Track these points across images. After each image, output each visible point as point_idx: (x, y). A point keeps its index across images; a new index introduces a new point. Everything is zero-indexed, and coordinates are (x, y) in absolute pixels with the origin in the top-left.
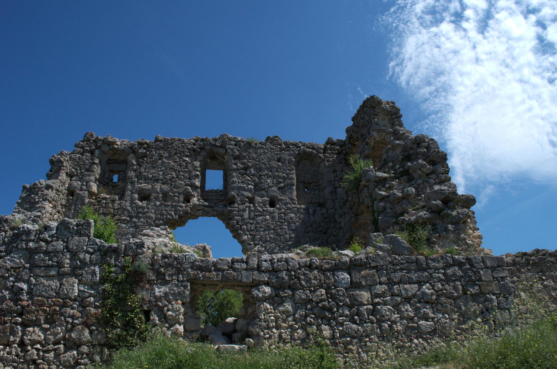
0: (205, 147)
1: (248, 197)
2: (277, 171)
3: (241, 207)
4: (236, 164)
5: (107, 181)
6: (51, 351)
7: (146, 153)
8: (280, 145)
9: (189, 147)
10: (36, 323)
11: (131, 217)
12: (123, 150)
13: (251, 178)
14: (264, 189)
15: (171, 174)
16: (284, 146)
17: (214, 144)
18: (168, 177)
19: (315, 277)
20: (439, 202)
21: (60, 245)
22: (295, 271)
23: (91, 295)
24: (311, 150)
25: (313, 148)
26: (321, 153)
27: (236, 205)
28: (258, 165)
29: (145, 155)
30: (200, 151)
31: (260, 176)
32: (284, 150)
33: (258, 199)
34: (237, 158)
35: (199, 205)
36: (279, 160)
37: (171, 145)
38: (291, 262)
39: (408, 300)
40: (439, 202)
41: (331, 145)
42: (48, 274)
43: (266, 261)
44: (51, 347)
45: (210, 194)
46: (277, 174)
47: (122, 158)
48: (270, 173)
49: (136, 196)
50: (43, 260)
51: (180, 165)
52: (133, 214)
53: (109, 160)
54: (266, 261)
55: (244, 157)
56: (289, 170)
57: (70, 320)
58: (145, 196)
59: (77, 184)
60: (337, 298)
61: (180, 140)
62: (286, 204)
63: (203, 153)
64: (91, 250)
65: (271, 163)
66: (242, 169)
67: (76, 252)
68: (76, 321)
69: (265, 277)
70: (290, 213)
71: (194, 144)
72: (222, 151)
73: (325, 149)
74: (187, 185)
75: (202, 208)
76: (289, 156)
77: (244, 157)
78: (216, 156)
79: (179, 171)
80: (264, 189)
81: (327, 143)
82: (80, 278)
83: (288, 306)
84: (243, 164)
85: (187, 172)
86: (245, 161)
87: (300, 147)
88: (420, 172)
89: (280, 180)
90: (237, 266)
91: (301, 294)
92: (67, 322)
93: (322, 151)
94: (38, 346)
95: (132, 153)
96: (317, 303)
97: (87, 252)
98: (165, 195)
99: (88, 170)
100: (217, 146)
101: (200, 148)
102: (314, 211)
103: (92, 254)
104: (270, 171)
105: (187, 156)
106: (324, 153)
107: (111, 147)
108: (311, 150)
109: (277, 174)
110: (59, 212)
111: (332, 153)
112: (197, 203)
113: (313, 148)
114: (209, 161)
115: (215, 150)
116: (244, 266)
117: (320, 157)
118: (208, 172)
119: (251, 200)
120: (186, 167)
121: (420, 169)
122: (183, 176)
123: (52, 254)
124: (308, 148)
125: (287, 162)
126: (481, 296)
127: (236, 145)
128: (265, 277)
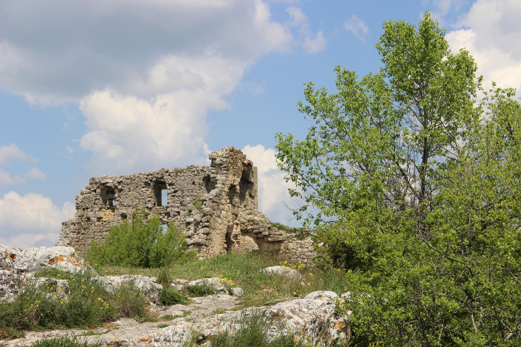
1: (177, 212)
2: (192, 192)
3: (173, 219)
9: (144, 181)
16: (196, 172)
27: (170, 218)
33: (182, 213)
36: (194, 183)
46: (192, 194)
49: (120, 218)
58: (124, 216)
59: (90, 214)
66: (173, 193)
84: (174, 189)
86: (174, 187)
89: (194, 198)
99: (94, 204)
105: (143, 187)
107: (105, 185)
109: (192, 194)
110: (83, 234)
114: (160, 185)
115: (159, 180)
119: (179, 213)
127: (169, 175)
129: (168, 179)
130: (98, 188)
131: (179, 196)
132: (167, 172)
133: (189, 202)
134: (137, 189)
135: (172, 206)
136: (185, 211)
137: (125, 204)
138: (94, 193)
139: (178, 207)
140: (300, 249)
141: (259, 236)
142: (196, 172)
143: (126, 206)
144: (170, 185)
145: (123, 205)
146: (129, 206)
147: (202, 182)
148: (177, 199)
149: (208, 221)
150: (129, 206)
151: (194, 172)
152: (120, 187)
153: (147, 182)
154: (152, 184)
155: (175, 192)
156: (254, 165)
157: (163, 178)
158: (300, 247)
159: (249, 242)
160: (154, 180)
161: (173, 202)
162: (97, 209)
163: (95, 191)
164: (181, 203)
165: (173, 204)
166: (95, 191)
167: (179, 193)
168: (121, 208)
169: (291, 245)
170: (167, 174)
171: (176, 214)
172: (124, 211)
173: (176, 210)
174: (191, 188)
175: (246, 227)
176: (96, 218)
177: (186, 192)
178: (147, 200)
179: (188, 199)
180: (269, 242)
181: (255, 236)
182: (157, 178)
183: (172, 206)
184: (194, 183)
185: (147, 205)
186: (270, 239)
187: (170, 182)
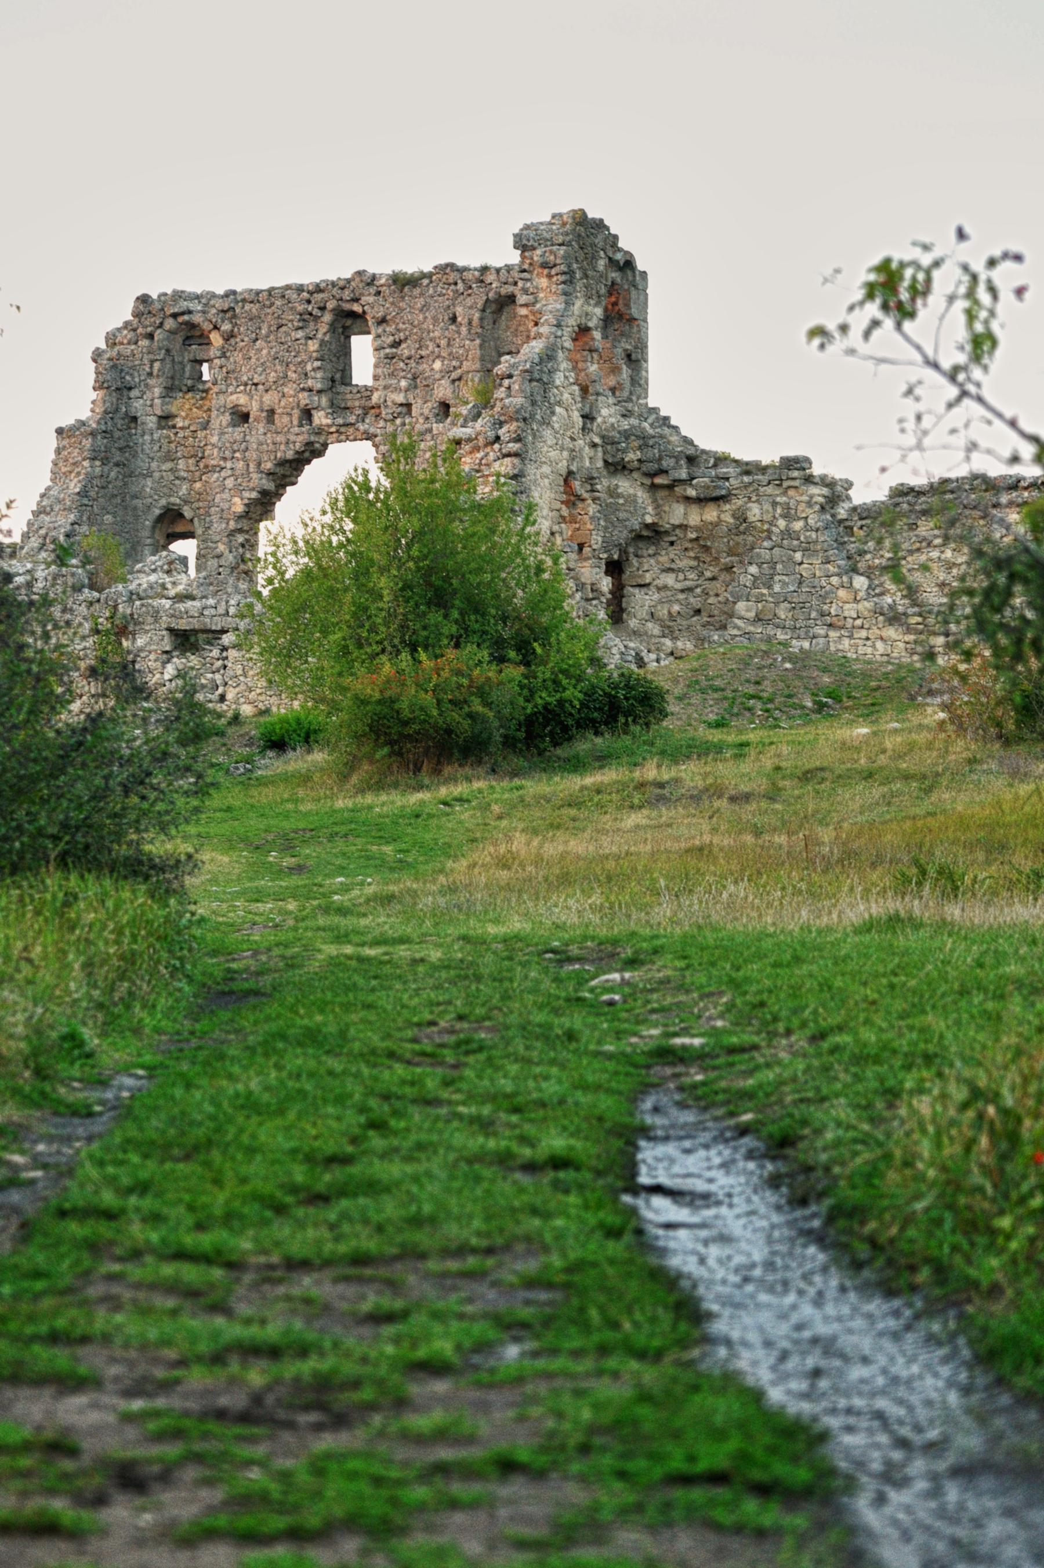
5: (190, 383)
9: (300, 308)
11: (225, 459)
16: (460, 286)
52: (228, 454)
53: (188, 338)
63: (327, 317)
71: (309, 302)
72: (356, 308)
98: (272, 412)
99: (150, 374)
114: (349, 322)
115: (347, 306)
116: (213, 611)
118: (354, 339)
127: (378, 293)
129: (370, 304)
135: (385, 388)
138: (144, 343)
140: (782, 523)
141: (658, 480)
142: (460, 286)
149: (518, 439)
155: (396, 344)
156: (640, 265)
158: (785, 516)
159: (631, 500)
160: (330, 305)
162: (157, 391)
163: (151, 336)
166: (151, 336)
169: (755, 512)
172: (242, 400)
173: (400, 398)
175: (620, 455)
176: (154, 419)
178: (309, 367)
180: (688, 499)
181: (648, 481)
184: (454, 319)
185: (310, 383)
186: (692, 492)
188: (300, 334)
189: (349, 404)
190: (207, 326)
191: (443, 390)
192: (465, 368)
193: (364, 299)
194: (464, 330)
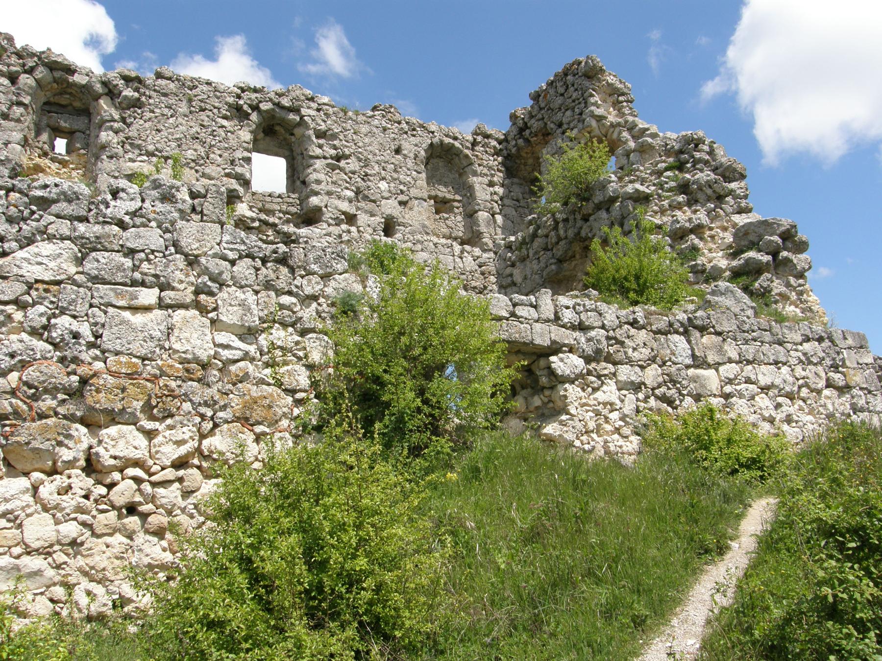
0: (261, 105)
1: (344, 213)
2: (395, 171)
4: (320, 146)
6: (170, 482)
7: (139, 99)
8: (399, 123)
9: (231, 100)
10: (113, 417)
12: (83, 86)
13: (350, 178)
14: (374, 201)
15: (195, 150)
17: (279, 103)
18: (190, 154)
19: (645, 344)
20: (776, 238)
21: (153, 238)
22: (614, 330)
23: (246, 357)
24: (451, 141)
25: (455, 139)
26: (467, 148)
28: (360, 153)
29: (136, 104)
30: (250, 111)
31: (366, 175)
32: (406, 133)
33: (363, 219)
34: (320, 135)
35: (253, 220)
36: (398, 151)
37: (191, 90)
38: (607, 312)
39: (765, 389)
40: (776, 238)
41: (484, 137)
42: (135, 303)
43: (567, 308)
44: (170, 474)
45: (268, 199)
46: (395, 175)
47: (77, 104)
48: (383, 172)
50: (120, 268)
51: (213, 134)
54: (567, 308)
55: (334, 136)
56: (415, 171)
57: (209, 413)
60: (680, 383)
61: (209, 83)
62: (412, 233)
64: (232, 255)
65: (385, 154)
66: (332, 158)
67: (196, 256)
68: (221, 414)
69: (568, 337)
70: (422, 250)
73: (474, 143)
74: (228, 175)
75: (257, 224)
76: (416, 145)
77: (334, 136)
78: (277, 128)
79: (211, 146)
80: (374, 201)
81: (475, 133)
82: (212, 315)
83: (609, 392)
85: (226, 149)
87: (433, 133)
88: (709, 192)
89: (401, 187)
90: (520, 311)
91: (625, 373)
92: (203, 416)
93: (470, 146)
94: (138, 472)
95: (107, 94)
96: (653, 389)
97: (224, 258)
100: (283, 108)
101: (250, 106)
102: (462, 252)
103: (233, 263)
104: (384, 170)
106: (473, 150)
107: (58, 74)
108: (451, 141)
109: (395, 175)
111: (486, 152)
112: (249, 214)
113: (455, 139)
117: (467, 156)
119: (351, 219)
120: (226, 139)
121: (710, 186)
122: (220, 156)
123: (142, 255)
124: (447, 136)
125: (412, 155)
126: (845, 390)
128: (568, 337)
130: (30, 71)
131: (354, 173)
132: (312, 99)
133: (386, 194)
134: (203, 116)
135: (329, 193)
136: (372, 215)
137: (151, 148)
139: (350, 201)
143: (150, 154)
144: (320, 135)
145: (139, 147)
146: (166, 158)
147: (423, 153)
148: (346, 177)
150: (166, 158)
151: (399, 123)
152: (128, 93)
153: (239, 108)
154: (254, 117)
155: (338, 158)
157: (296, 110)
161: (334, 183)
164: (358, 192)
165: (331, 188)
167: (352, 164)
168: (130, 155)
170: (314, 105)
171: (343, 217)
173: (345, 206)
174: (393, 160)
177: (376, 167)
179: (383, 185)
182: (278, 105)
183: (329, 193)
184: (398, 151)
185: (239, 170)
187: (323, 127)
188: (225, 123)
189: (267, 206)
190: (98, 88)
191: (390, 207)
192: (414, 192)
193: (304, 111)
194: (410, 163)
